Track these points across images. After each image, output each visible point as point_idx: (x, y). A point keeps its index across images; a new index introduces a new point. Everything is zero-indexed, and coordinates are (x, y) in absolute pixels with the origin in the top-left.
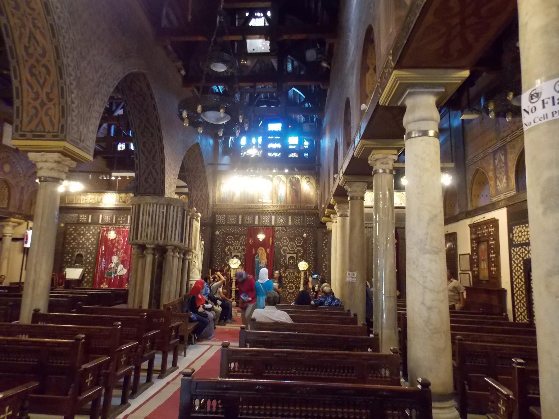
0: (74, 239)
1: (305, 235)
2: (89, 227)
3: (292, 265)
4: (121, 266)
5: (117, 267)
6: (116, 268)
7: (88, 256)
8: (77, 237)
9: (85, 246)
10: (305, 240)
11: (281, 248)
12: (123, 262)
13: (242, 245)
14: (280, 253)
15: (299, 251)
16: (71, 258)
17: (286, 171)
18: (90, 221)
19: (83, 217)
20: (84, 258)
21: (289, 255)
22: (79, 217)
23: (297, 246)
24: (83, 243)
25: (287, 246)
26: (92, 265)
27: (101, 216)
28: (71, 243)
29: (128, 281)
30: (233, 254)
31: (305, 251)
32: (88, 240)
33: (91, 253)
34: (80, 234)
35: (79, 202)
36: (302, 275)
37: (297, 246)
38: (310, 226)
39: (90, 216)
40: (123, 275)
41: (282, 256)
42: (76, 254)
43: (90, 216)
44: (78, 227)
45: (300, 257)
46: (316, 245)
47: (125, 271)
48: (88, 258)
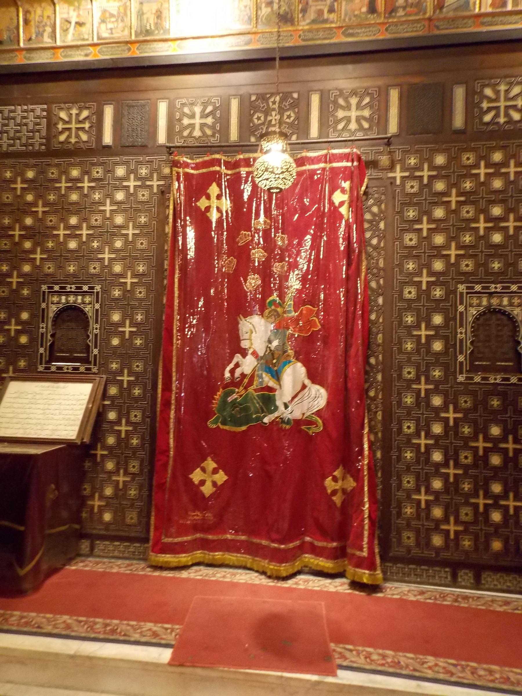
0: (39, 234)
2: (109, 171)
4: (294, 373)
5: (277, 376)
6: (268, 380)
7: (116, 317)
8: (52, 220)
9: (94, 268)
12: (306, 351)
16: (27, 328)
18: (108, 139)
19: (72, 121)
20: (95, 328)
22: (51, 124)
24: (85, 255)
26: (138, 366)
27: (163, 108)
28: (25, 256)
29: (348, 460)
32: (107, 233)
33: (126, 304)
34: (63, 209)
35: (47, 41)
39: (109, 112)
40: (309, 422)
42: (54, 308)
43: (109, 112)
44: (53, 173)
47: (318, 397)
48: (113, 329)
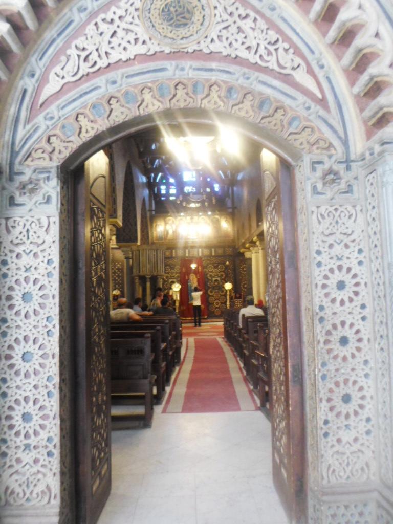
1: (227, 263)
3: (216, 286)
10: (227, 267)
11: (207, 274)
13: (177, 273)
14: (208, 278)
15: (222, 275)
17: (210, 213)
21: (214, 279)
23: (220, 272)
25: (212, 272)
30: (170, 280)
31: (227, 276)
36: (228, 293)
37: (220, 272)
38: (230, 256)
41: (209, 280)
45: (222, 279)
46: (234, 270)
